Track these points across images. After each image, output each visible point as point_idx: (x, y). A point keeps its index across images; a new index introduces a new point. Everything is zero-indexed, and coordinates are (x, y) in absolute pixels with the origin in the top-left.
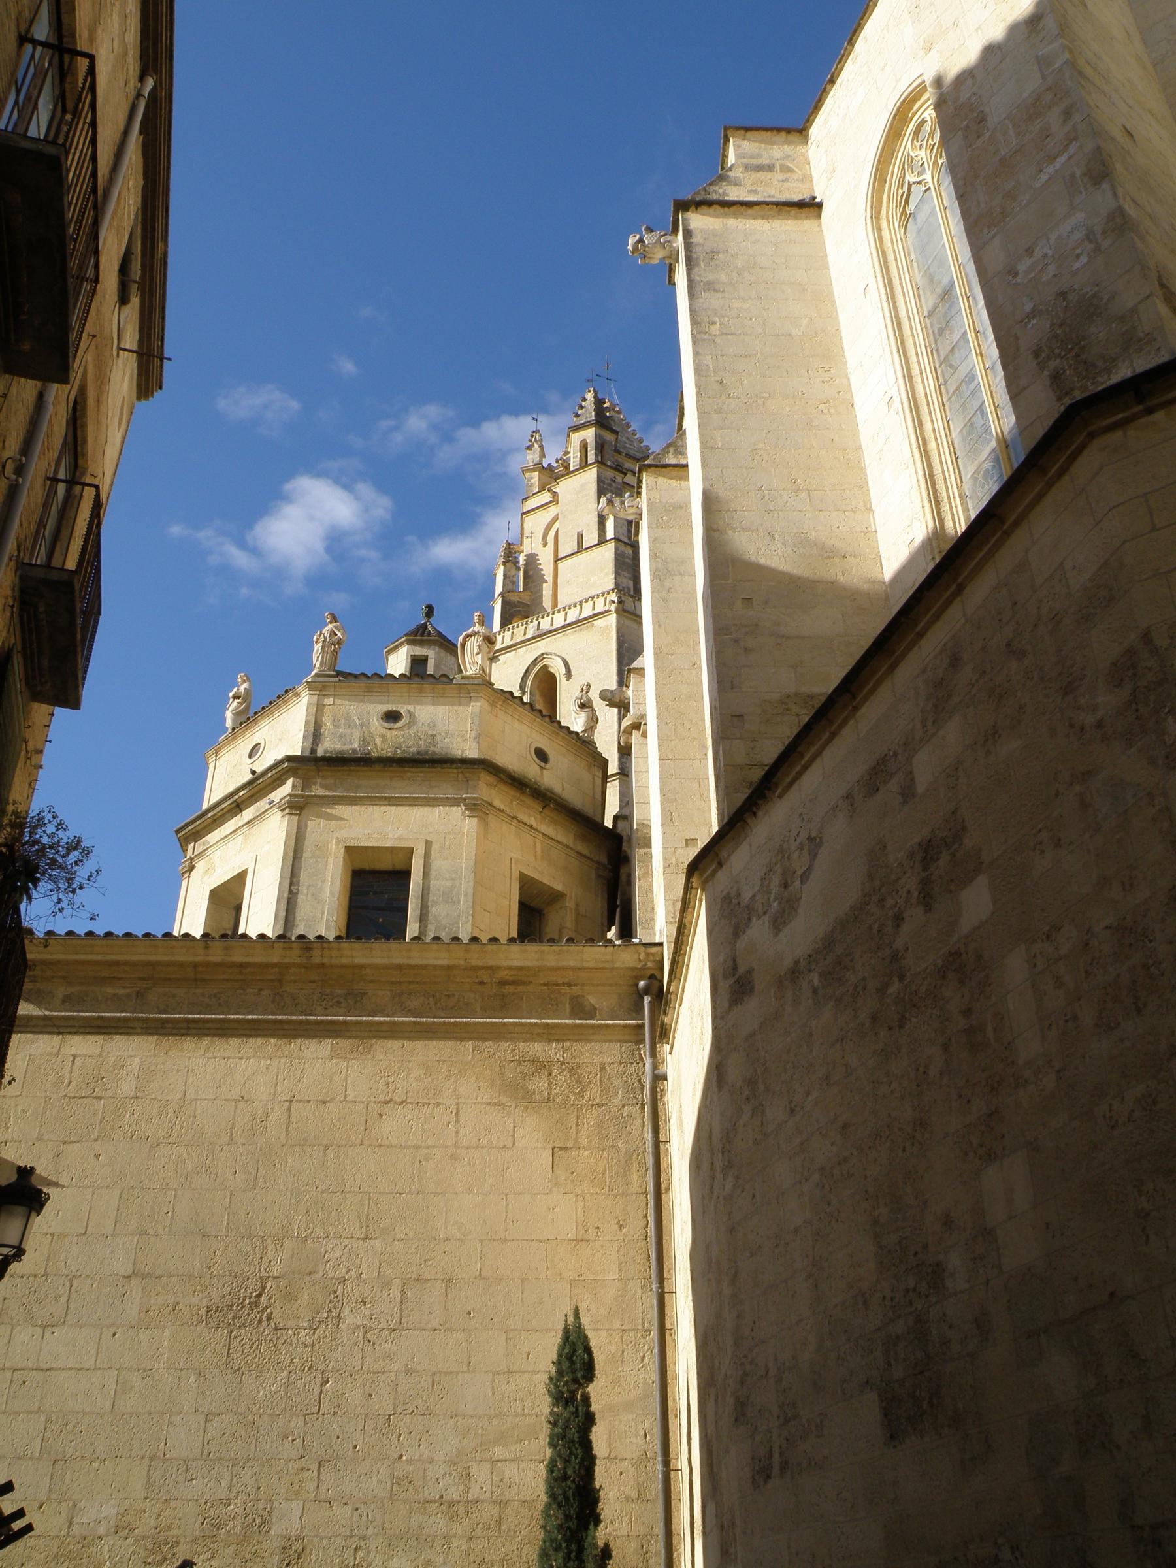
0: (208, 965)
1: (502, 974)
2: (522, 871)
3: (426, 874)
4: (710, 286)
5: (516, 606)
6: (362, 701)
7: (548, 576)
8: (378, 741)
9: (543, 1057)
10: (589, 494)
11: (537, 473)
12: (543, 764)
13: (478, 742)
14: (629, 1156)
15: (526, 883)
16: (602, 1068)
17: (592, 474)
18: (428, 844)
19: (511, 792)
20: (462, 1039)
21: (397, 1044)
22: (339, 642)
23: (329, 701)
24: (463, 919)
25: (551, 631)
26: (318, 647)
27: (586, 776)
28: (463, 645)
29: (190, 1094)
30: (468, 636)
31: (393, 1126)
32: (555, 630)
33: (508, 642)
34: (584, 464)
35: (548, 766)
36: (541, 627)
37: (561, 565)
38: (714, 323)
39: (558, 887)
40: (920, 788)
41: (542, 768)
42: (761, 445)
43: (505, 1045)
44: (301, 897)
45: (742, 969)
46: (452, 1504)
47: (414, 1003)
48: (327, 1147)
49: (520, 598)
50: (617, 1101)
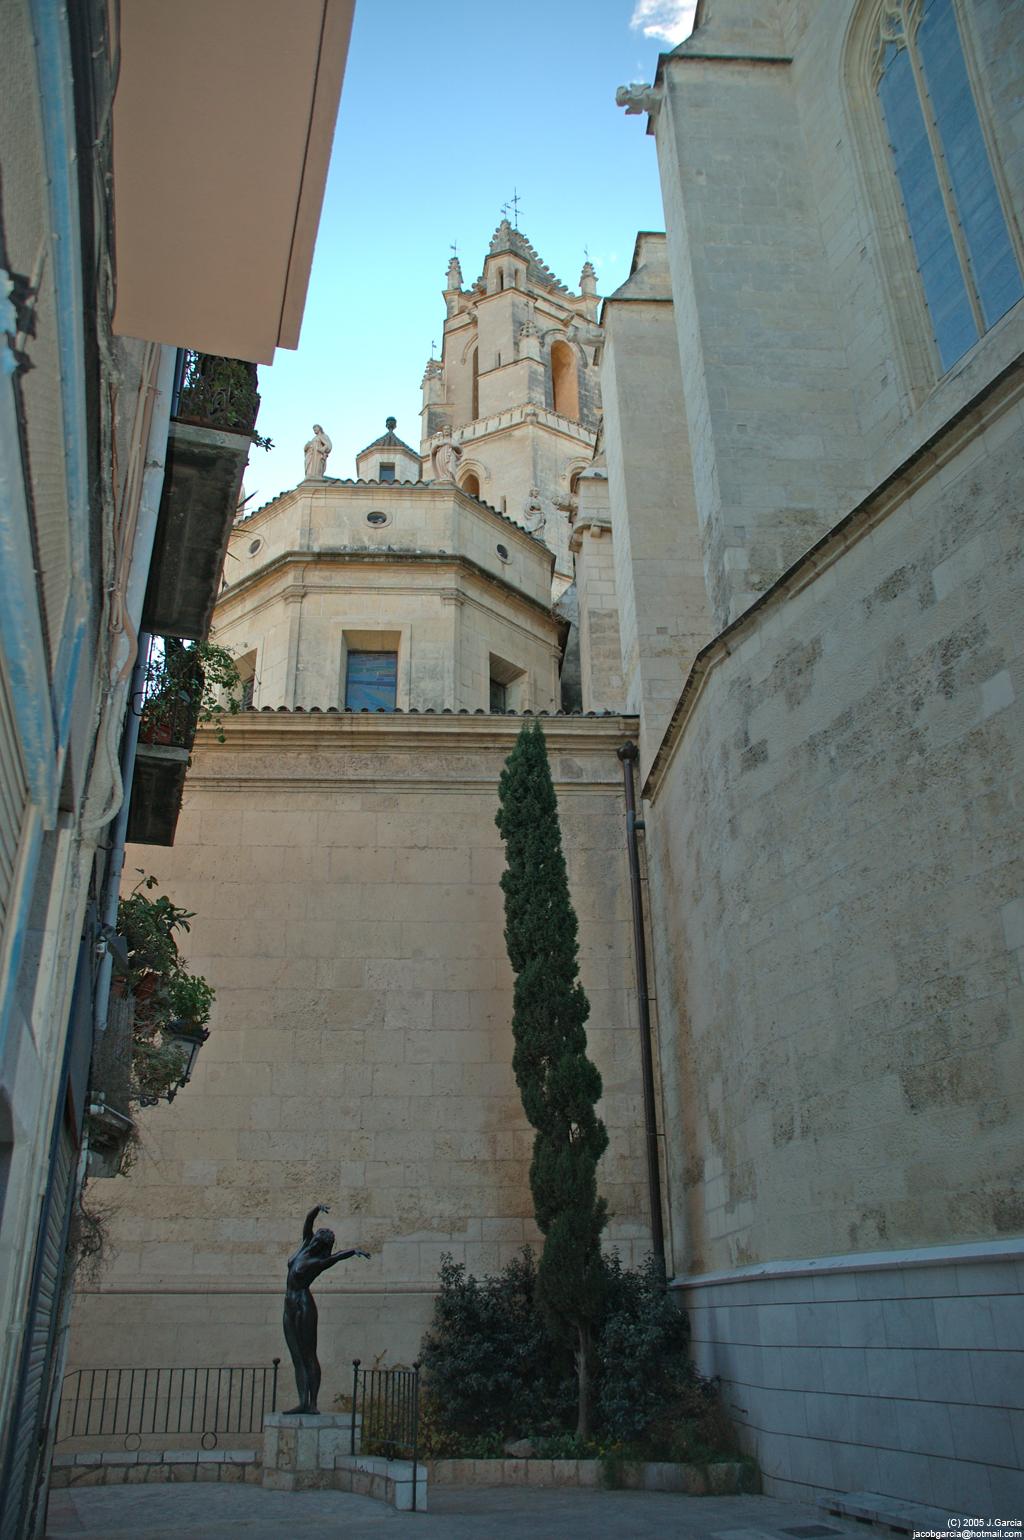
2: (494, 652)
12: (504, 560)
25: (473, 440)
32: (477, 439)
39: (520, 665)
40: (940, 596)
41: (504, 563)
45: (754, 741)
46: (484, 1162)
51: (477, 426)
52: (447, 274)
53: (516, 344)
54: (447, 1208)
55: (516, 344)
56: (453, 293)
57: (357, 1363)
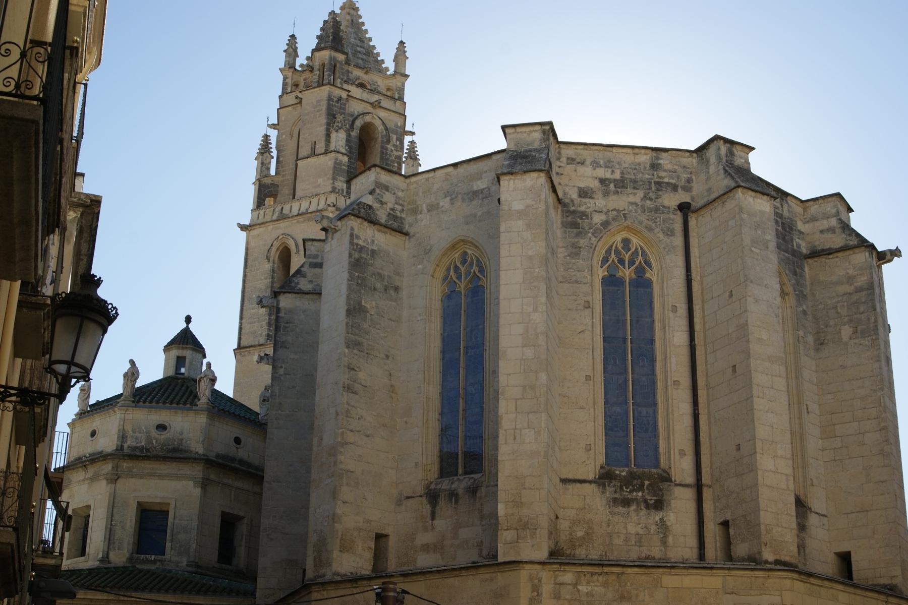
2: (224, 510)
10: (322, 110)
12: (238, 446)
13: (203, 444)
37: (299, 163)
38: (281, 367)
39: (242, 514)
41: (237, 448)
49: (272, 181)
51: (293, 204)
52: (285, 51)
53: (328, 135)
55: (328, 135)
56: (290, 65)
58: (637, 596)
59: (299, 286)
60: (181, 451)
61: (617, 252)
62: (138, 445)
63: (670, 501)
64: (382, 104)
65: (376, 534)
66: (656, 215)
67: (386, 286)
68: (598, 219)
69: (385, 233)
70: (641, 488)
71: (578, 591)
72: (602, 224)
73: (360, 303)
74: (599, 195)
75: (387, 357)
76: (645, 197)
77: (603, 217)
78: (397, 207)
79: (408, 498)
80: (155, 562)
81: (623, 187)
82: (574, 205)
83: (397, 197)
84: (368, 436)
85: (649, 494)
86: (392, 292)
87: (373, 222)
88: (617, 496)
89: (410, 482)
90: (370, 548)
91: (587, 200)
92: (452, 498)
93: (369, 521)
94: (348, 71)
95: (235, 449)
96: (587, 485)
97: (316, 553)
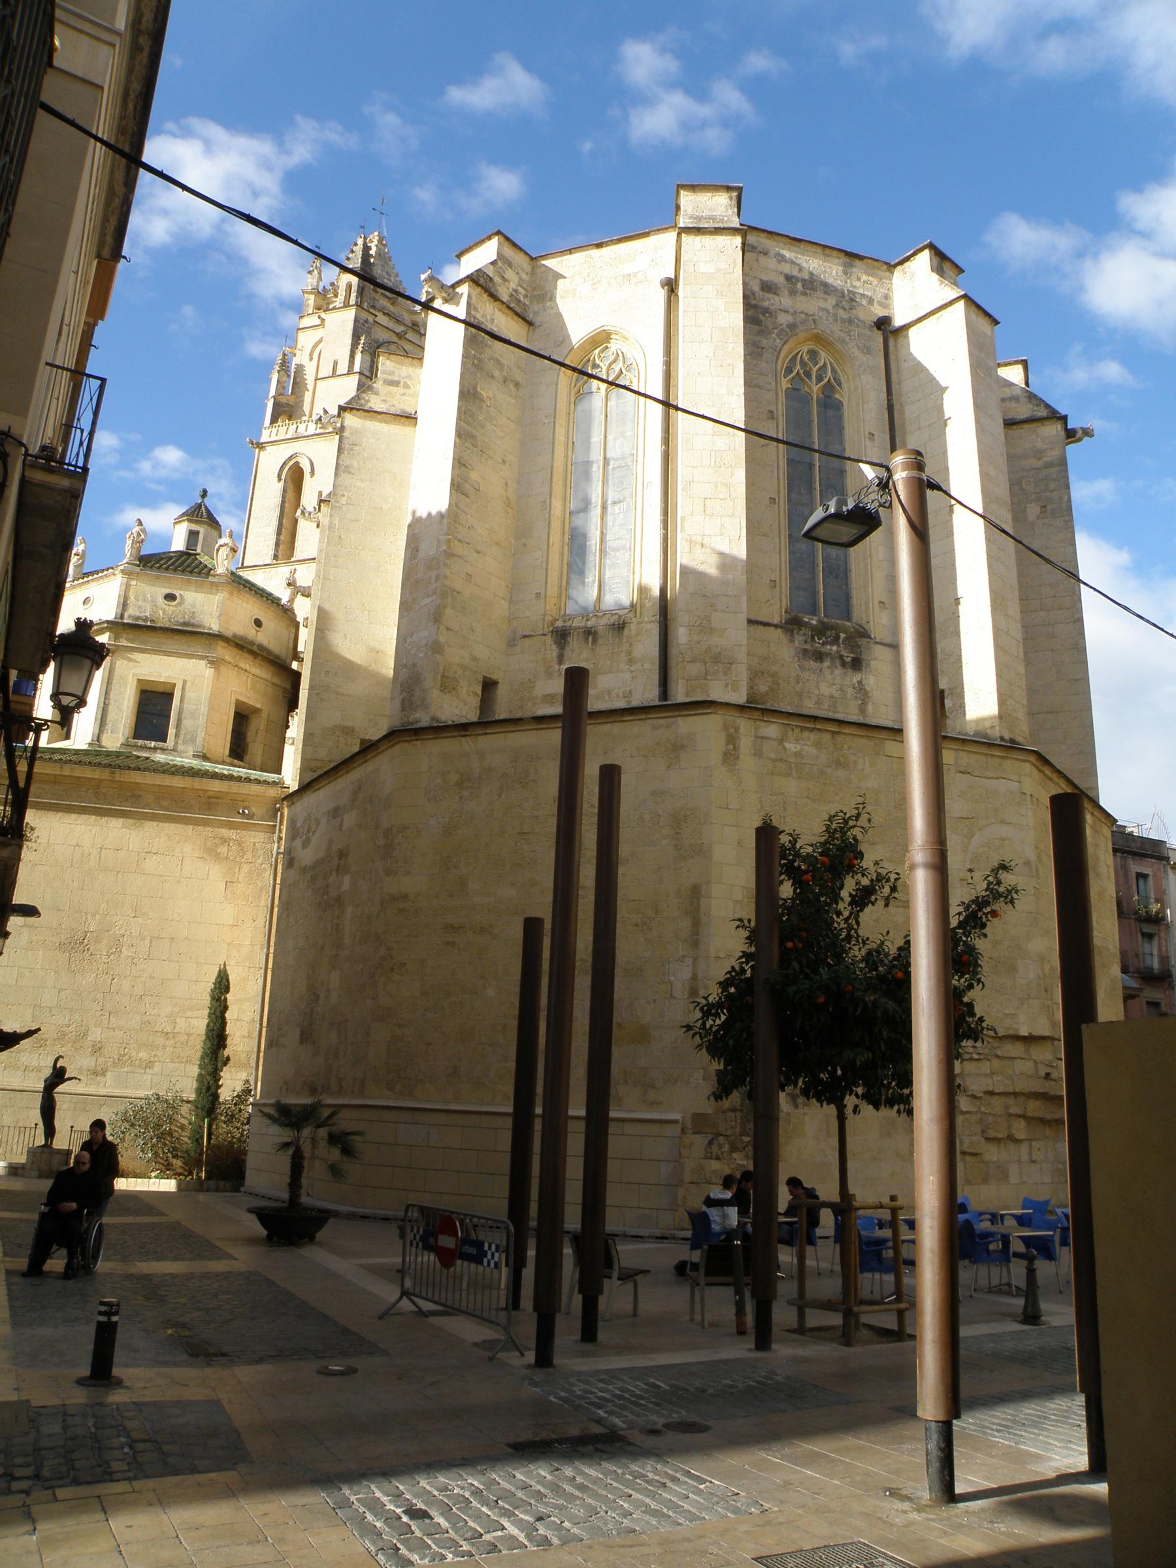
0: (62, 775)
1: (209, 793)
3: (182, 700)
4: (347, 469)
5: (283, 406)
6: (154, 585)
7: (310, 386)
8: (161, 612)
9: (226, 836)
11: (313, 297)
14: (262, 889)
15: (239, 704)
16: (254, 844)
17: (350, 314)
18: (185, 682)
19: (236, 651)
20: (187, 824)
21: (155, 824)
22: (142, 541)
23: (133, 583)
24: (200, 729)
26: (129, 542)
27: (286, 632)
28: (218, 550)
29: (51, 841)
30: (221, 546)
31: (151, 864)
33: (273, 438)
34: (346, 305)
35: (261, 629)
36: (299, 431)
38: (343, 496)
39: (258, 706)
40: (344, 829)
42: (352, 580)
43: (208, 829)
44: (110, 707)
47: (165, 803)
48: (118, 872)
50: (260, 861)
54: (143, 1055)
57: (72, 1127)
58: (855, 762)
59: (370, 405)
60: (193, 625)
61: (803, 364)
62: (141, 615)
63: (869, 661)
64: (407, 336)
65: (484, 677)
66: (850, 328)
67: (505, 377)
68: (783, 319)
69: (507, 315)
70: (836, 640)
71: (785, 749)
72: (788, 326)
73: (475, 388)
74: (785, 292)
75: (504, 462)
76: (837, 305)
77: (790, 319)
78: (520, 289)
79: (525, 637)
80: (155, 749)
81: (812, 289)
82: (755, 299)
83: (520, 278)
84: (478, 552)
85: (845, 649)
86: (512, 386)
87: (494, 297)
88: (808, 647)
89: (528, 617)
90: (476, 694)
91: (771, 296)
92: (588, 638)
93: (474, 659)
94: (374, 299)
95: (254, 632)
96: (772, 629)
97: (405, 694)
